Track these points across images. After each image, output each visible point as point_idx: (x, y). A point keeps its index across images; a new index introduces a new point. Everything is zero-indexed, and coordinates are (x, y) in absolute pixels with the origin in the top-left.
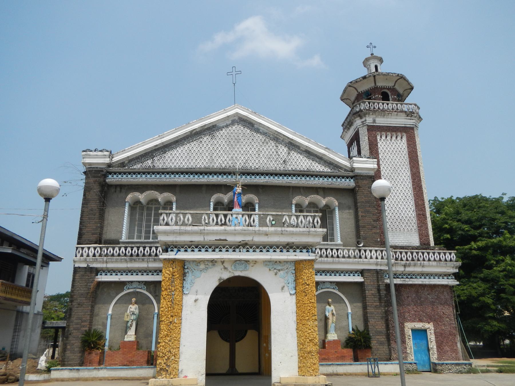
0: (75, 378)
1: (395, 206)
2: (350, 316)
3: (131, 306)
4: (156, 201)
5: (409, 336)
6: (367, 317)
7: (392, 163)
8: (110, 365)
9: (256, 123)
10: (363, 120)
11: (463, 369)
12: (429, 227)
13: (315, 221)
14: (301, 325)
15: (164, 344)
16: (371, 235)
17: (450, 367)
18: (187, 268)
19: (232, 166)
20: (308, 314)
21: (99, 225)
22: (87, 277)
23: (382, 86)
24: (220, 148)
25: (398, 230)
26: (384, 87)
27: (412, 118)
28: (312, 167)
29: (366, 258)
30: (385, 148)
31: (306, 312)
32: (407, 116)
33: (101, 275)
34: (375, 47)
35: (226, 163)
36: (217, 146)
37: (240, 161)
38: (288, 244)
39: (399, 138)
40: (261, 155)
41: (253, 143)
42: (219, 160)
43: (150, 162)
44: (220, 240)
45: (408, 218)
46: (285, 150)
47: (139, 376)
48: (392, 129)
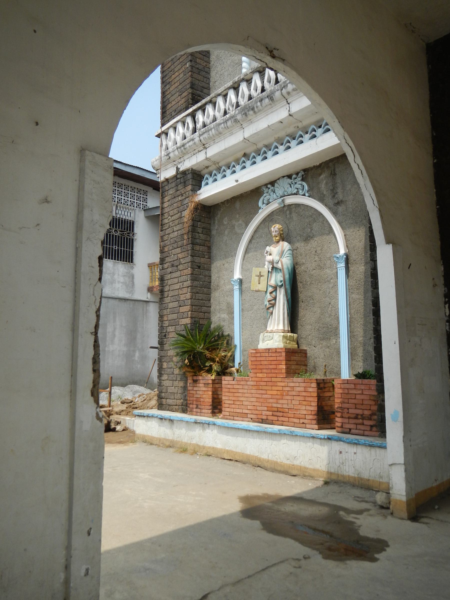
8: (233, 416)
33: (207, 184)
47: (288, 462)
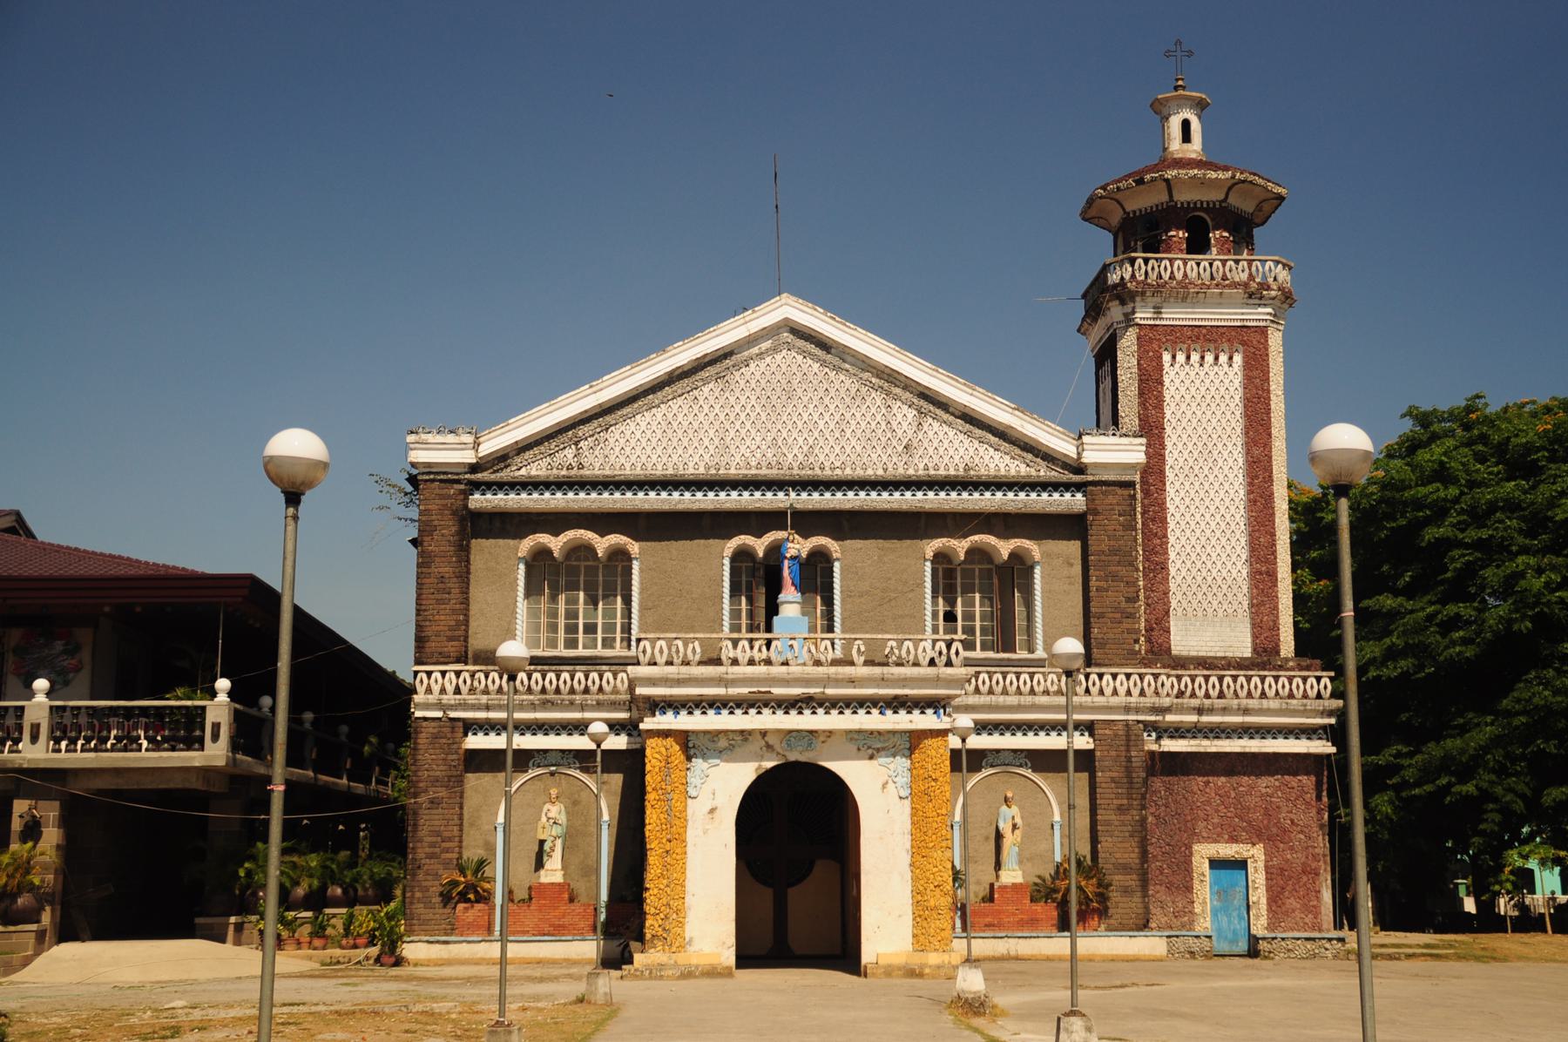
0: (441, 959)
1: (1198, 550)
2: (1057, 827)
3: (547, 806)
4: (589, 549)
5: (1204, 875)
6: (1097, 831)
7: (1200, 430)
9: (835, 345)
10: (1128, 309)
11: (1323, 950)
12: (1280, 607)
13: (953, 651)
14: (919, 858)
15: (656, 891)
16: (1117, 636)
17: (1290, 947)
18: (694, 747)
19: (774, 464)
20: (934, 836)
21: (461, 617)
22: (444, 741)
23: (1189, 203)
24: (743, 416)
25: (1200, 614)
26: (1195, 203)
27: (1262, 302)
28: (977, 461)
29: (1101, 692)
30: (1183, 390)
31: (930, 832)
32: (1250, 297)
34: (1190, 54)
35: (758, 455)
36: (737, 409)
37: (796, 451)
38: (896, 697)
39: (1223, 358)
40: (848, 432)
41: (827, 401)
42: (743, 448)
43: (570, 453)
44: (760, 692)
45: (1229, 582)
46: (910, 416)
48: (1204, 336)
